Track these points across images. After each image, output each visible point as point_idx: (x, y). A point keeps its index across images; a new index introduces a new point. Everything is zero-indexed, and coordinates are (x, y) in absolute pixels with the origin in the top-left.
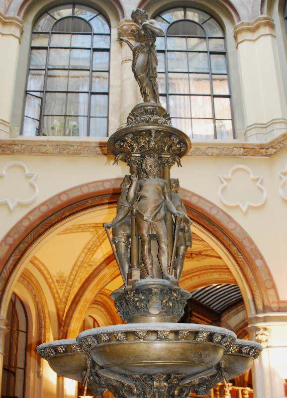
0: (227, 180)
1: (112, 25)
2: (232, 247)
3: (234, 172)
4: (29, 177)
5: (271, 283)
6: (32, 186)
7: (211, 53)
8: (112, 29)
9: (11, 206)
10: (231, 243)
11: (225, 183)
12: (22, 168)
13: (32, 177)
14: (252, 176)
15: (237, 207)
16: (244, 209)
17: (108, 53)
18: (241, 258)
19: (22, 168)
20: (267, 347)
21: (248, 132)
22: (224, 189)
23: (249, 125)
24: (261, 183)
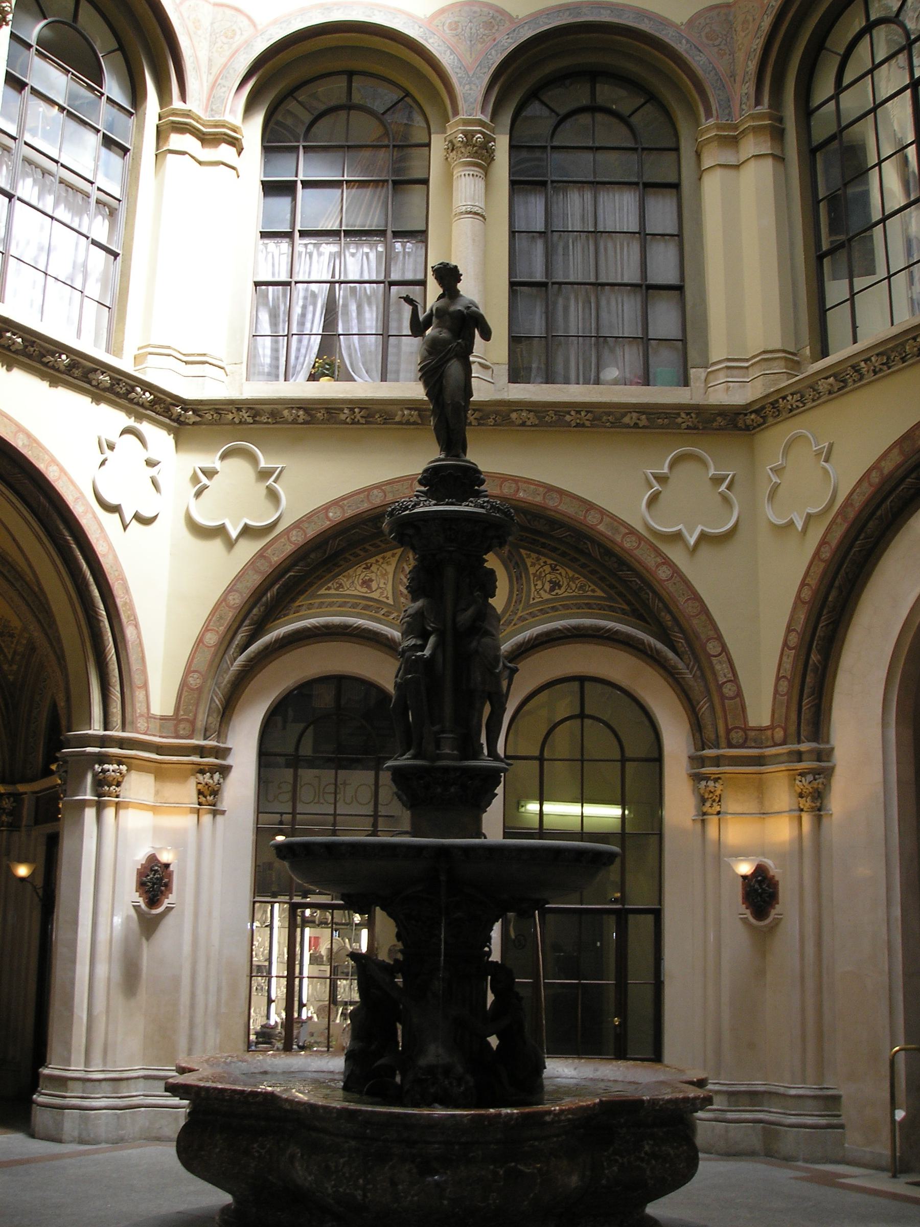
0: (662, 479)
1: (432, 131)
2: (663, 614)
3: (672, 466)
4: (264, 474)
5: (735, 688)
6: (273, 495)
7: (647, 185)
8: (433, 136)
9: (234, 533)
10: (661, 605)
11: (657, 487)
12: (253, 459)
13: (274, 473)
14: (712, 472)
15: (677, 537)
16: (692, 541)
17: (424, 186)
18: (680, 638)
19: (253, 459)
20: (719, 813)
21: (711, 377)
22: (653, 500)
23: (714, 359)
24: (728, 488)
